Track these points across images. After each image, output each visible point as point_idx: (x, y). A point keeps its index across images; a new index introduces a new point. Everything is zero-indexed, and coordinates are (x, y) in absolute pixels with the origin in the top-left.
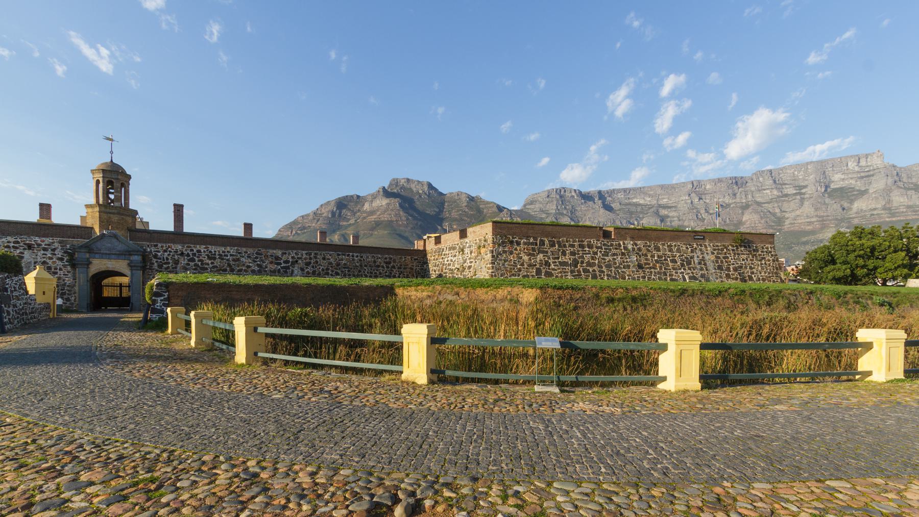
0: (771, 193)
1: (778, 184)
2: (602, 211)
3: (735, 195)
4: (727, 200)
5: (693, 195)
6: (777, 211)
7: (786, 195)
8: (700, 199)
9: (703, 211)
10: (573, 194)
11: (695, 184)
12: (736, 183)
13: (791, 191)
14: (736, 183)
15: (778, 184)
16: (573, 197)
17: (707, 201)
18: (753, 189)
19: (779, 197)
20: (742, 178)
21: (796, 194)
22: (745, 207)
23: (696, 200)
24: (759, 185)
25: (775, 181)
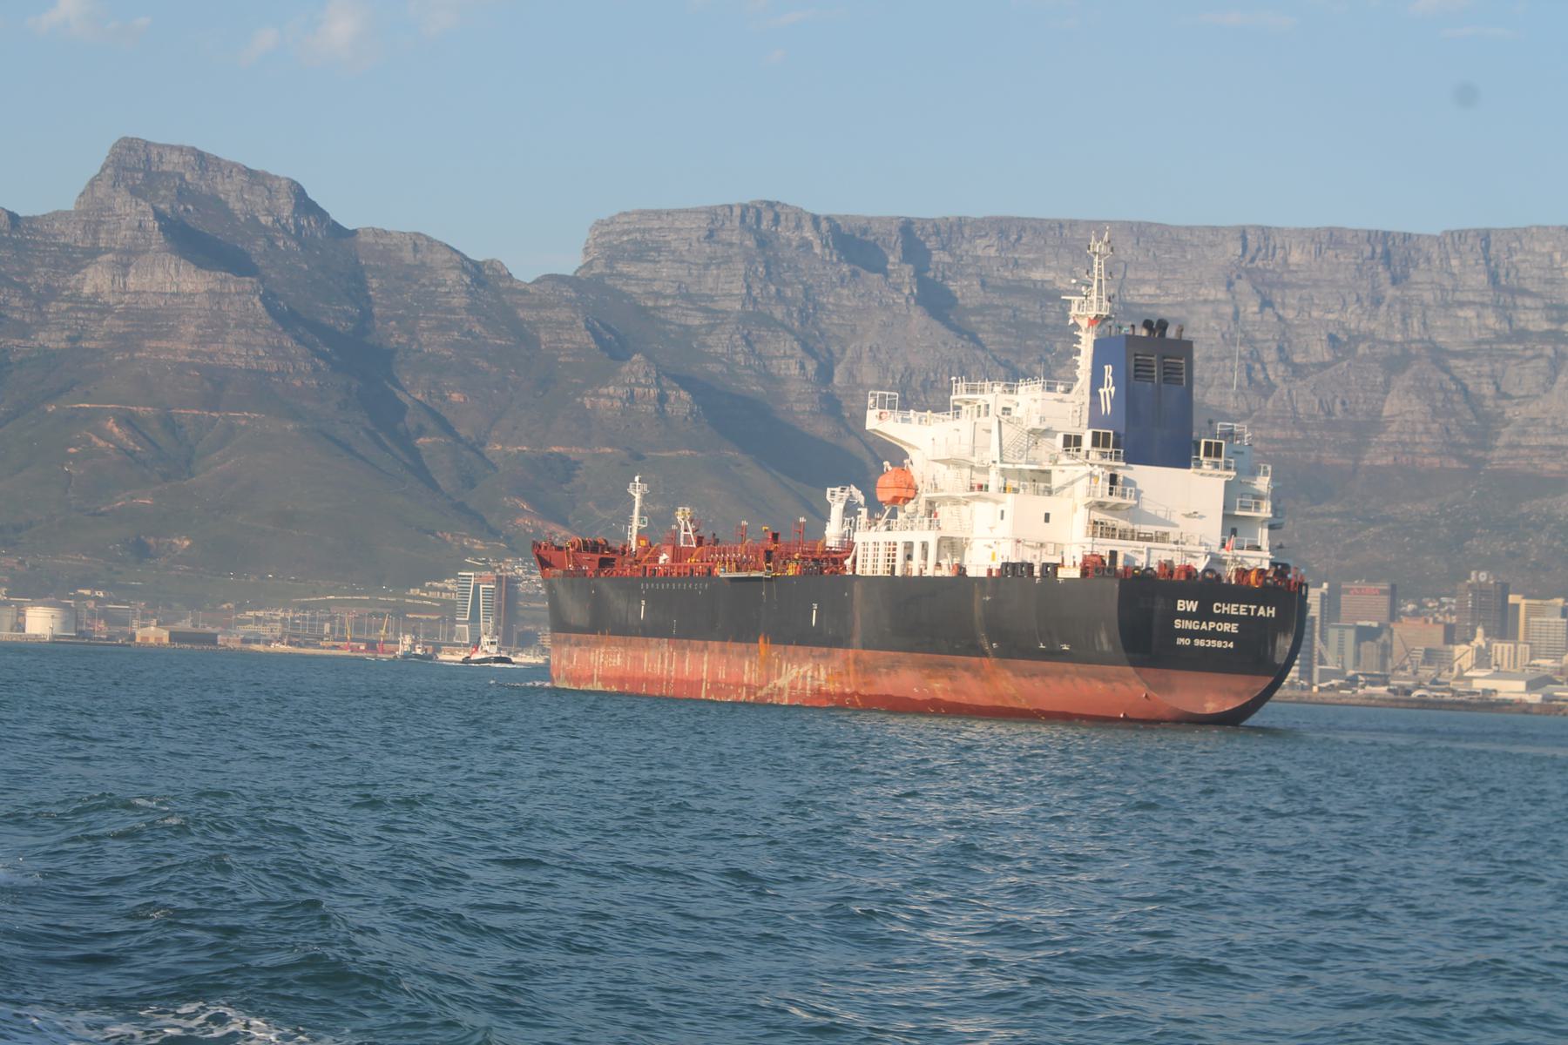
0: (1478, 322)
1: (1504, 290)
2: (919, 318)
3: (1377, 302)
4: (1353, 319)
5: (1243, 286)
6: (1488, 390)
7: (1521, 335)
8: (1266, 303)
9: (1270, 355)
10: (809, 234)
11: (1253, 245)
12: (1387, 255)
13: (1535, 321)
14: (1387, 255)
15: (1504, 290)
16: (806, 245)
17: (1290, 314)
18: (1428, 297)
19: (1500, 337)
20: (1407, 237)
21: (1545, 337)
22: (1396, 363)
23: (1253, 307)
24: (1448, 284)
25: (1494, 278)
